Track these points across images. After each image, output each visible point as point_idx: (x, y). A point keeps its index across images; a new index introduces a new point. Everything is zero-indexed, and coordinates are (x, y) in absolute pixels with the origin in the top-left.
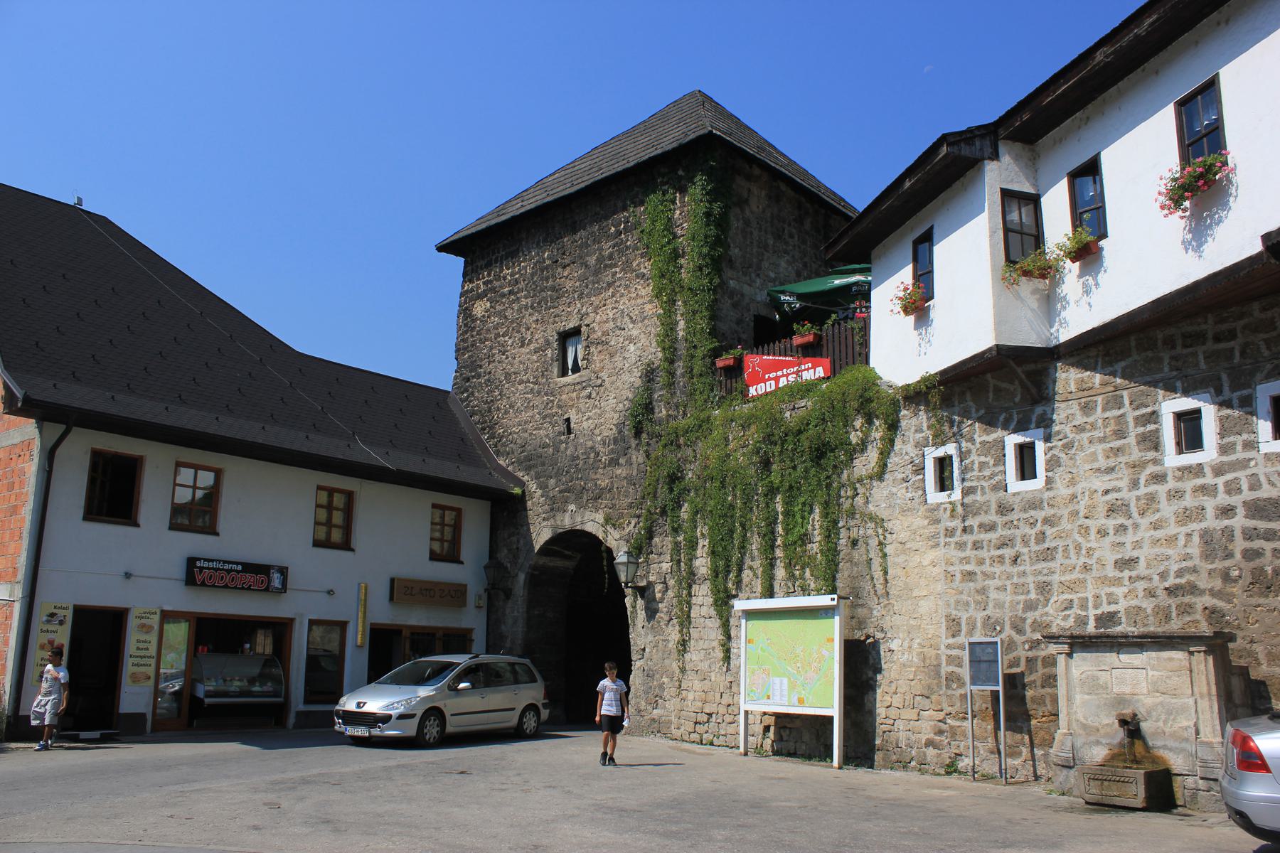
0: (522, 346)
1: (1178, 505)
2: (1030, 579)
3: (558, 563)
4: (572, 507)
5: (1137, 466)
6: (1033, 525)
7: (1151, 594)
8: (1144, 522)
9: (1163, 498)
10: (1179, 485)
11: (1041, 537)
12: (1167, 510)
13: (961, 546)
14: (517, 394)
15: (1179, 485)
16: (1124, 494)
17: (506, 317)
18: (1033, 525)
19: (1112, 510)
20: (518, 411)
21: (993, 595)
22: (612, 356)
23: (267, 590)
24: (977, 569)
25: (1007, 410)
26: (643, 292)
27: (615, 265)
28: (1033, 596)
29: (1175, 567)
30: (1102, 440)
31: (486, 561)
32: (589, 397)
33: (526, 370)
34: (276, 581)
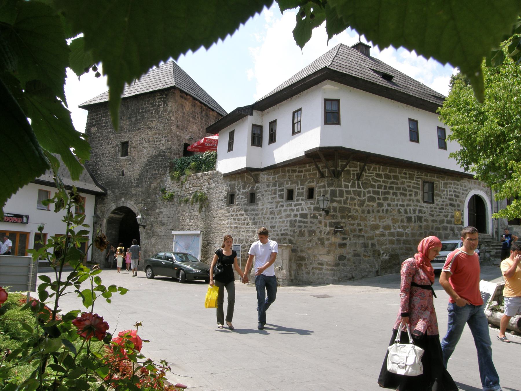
0: (108, 145)
1: (286, 213)
2: (251, 229)
3: (117, 216)
4: (123, 199)
5: (278, 202)
6: (252, 215)
7: (277, 235)
8: (278, 217)
9: (283, 211)
10: (287, 208)
11: (254, 219)
12: (283, 214)
13: (235, 219)
14: (106, 160)
15: (287, 208)
16: (274, 209)
17: (103, 134)
18: (252, 215)
19: (271, 213)
20: (106, 166)
21: (241, 233)
22: (138, 152)
23: (22, 223)
24: (238, 226)
25: (249, 184)
26: (150, 133)
27: (141, 123)
28: (251, 234)
29: (283, 229)
30: (271, 195)
31: (93, 215)
32: (130, 164)
33: (109, 153)
34: (25, 220)
